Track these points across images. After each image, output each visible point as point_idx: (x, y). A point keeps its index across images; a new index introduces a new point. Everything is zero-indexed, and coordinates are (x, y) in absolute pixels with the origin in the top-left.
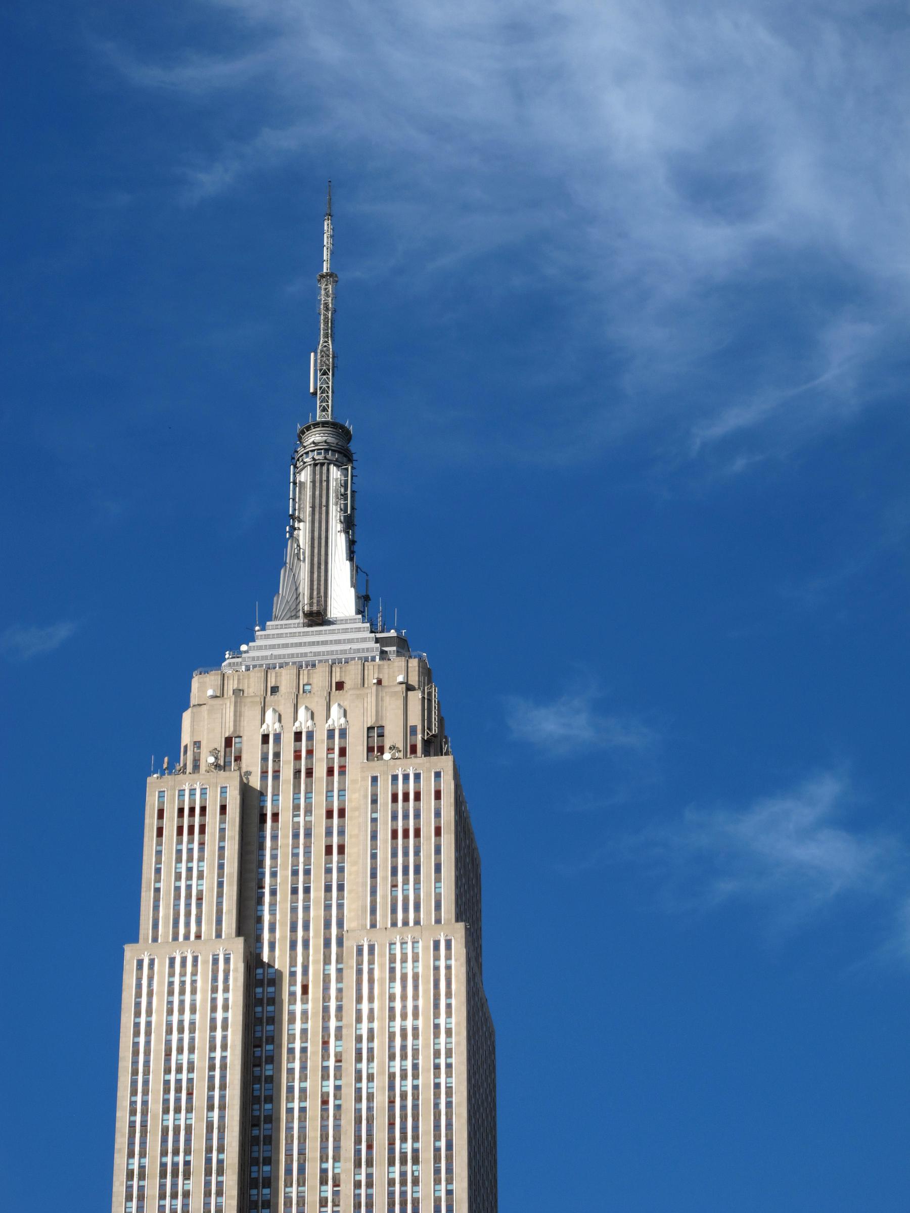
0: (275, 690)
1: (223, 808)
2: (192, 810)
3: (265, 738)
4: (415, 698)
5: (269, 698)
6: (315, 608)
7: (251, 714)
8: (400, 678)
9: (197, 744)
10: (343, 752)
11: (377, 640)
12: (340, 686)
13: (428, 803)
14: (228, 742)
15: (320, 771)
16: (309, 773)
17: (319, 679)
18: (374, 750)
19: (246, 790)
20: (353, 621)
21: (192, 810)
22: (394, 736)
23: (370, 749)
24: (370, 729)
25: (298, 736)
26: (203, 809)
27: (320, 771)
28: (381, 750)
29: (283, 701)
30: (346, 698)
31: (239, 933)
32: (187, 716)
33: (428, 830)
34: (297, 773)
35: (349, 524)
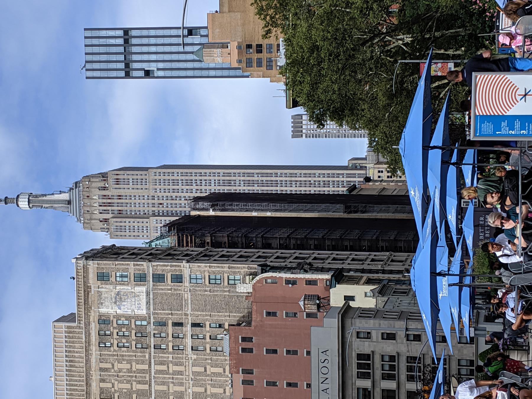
0: (88, 211)
3: (101, 213)
6: (67, 203)
7: (94, 216)
8: (87, 183)
11: (76, 188)
12: (88, 197)
14: (101, 221)
15: (109, 201)
16: (110, 203)
18: (105, 188)
19: (113, 218)
20: (70, 194)
22: (102, 184)
24: (99, 190)
25: (100, 206)
27: (109, 201)
30: (91, 195)
34: (109, 206)
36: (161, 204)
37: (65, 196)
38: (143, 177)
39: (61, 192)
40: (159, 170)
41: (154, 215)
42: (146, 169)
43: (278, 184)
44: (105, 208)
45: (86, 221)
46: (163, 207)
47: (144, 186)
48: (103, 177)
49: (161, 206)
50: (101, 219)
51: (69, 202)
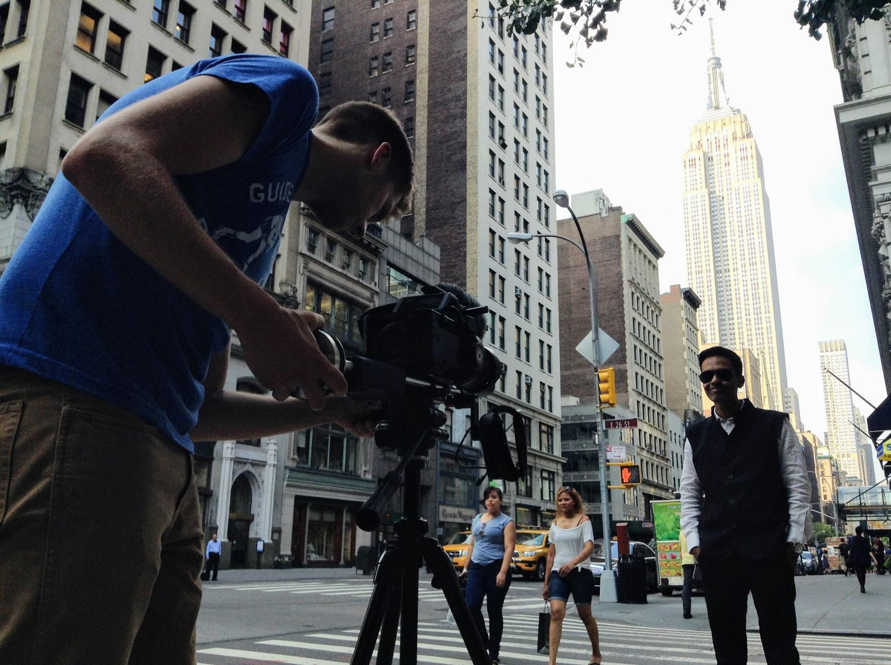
0: (709, 127)
3: (708, 140)
4: (743, 124)
12: (725, 124)
13: (749, 148)
14: (699, 142)
15: (722, 145)
16: (719, 147)
17: (720, 123)
18: (735, 139)
22: (739, 135)
29: (711, 130)
33: (749, 157)
36: (723, 198)
37: (723, 103)
38: (751, 175)
40: (760, 192)
41: (710, 193)
42: (761, 174)
43: (758, 315)
44: (714, 143)
45: (698, 128)
46: (720, 201)
47: (740, 177)
48: (747, 135)
49: (721, 198)
50: (701, 142)
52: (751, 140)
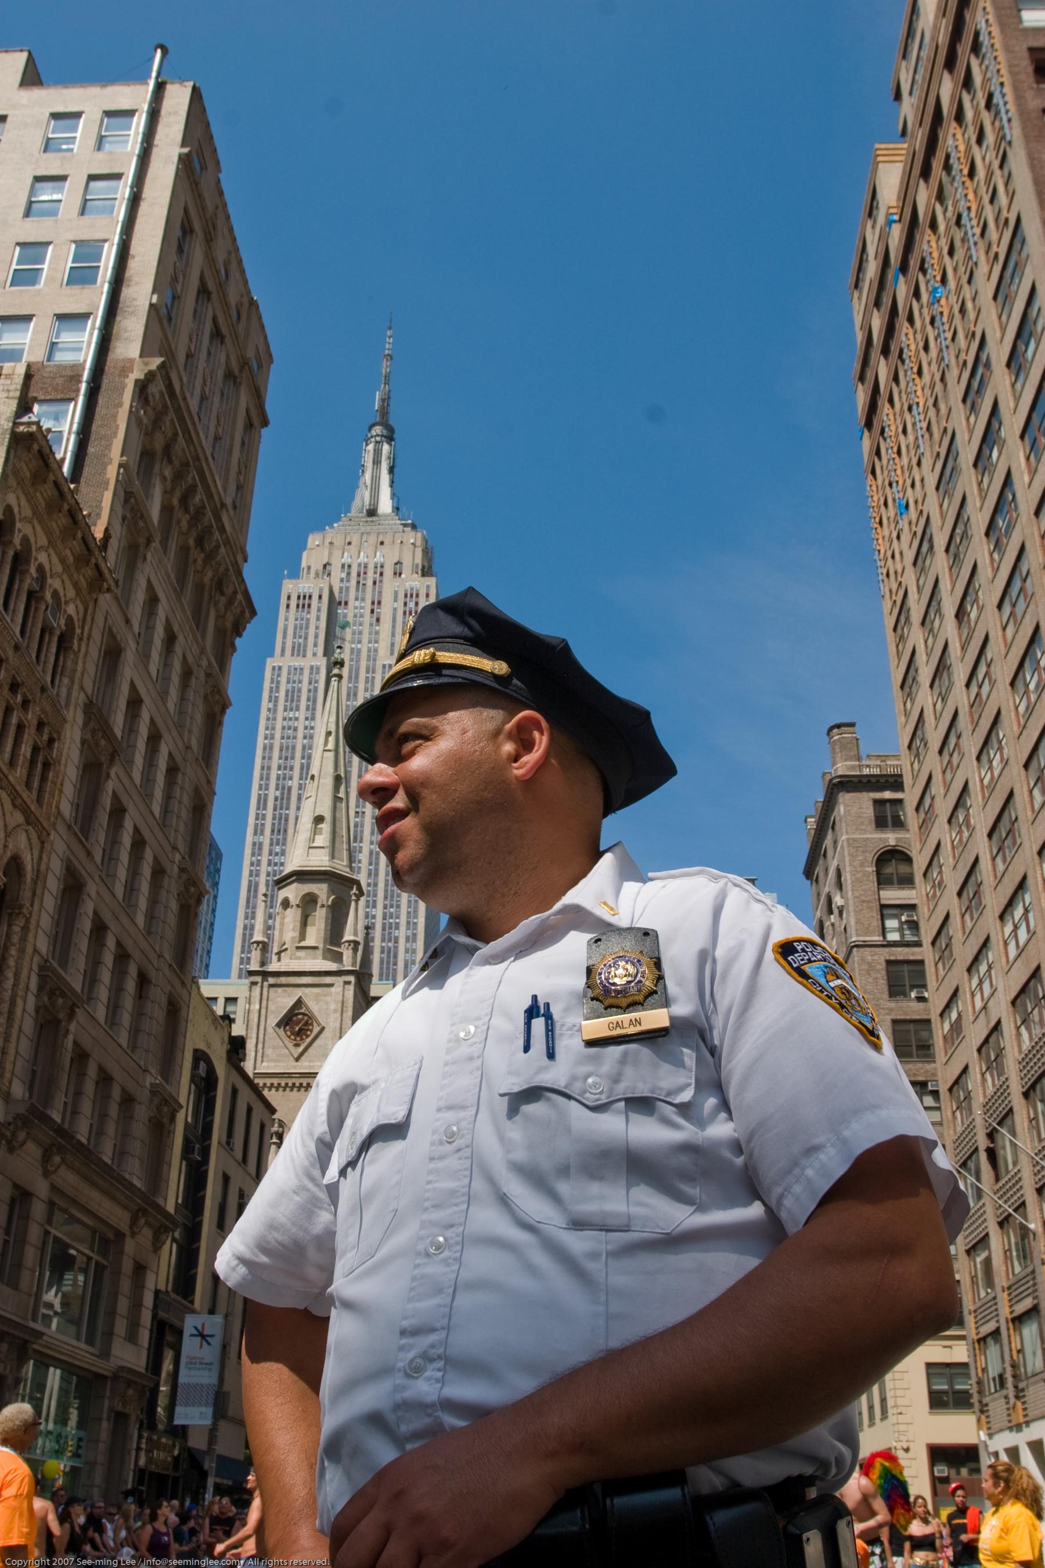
0: (349, 543)
1: (320, 597)
2: (304, 597)
3: (343, 566)
5: (347, 547)
7: (337, 553)
8: (412, 541)
9: (309, 568)
10: (381, 574)
12: (382, 543)
14: (325, 566)
18: (398, 574)
21: (304, 597)
23: (395, 574)
24: (396, 564)
26: (310, 597)
28: (400, 574)
30: (385, 549)
31: (325, 655)
32: (305, 554)
35: (391, 470)
39: (393, 496)
51: (372, 512)
52: (432, 581)
